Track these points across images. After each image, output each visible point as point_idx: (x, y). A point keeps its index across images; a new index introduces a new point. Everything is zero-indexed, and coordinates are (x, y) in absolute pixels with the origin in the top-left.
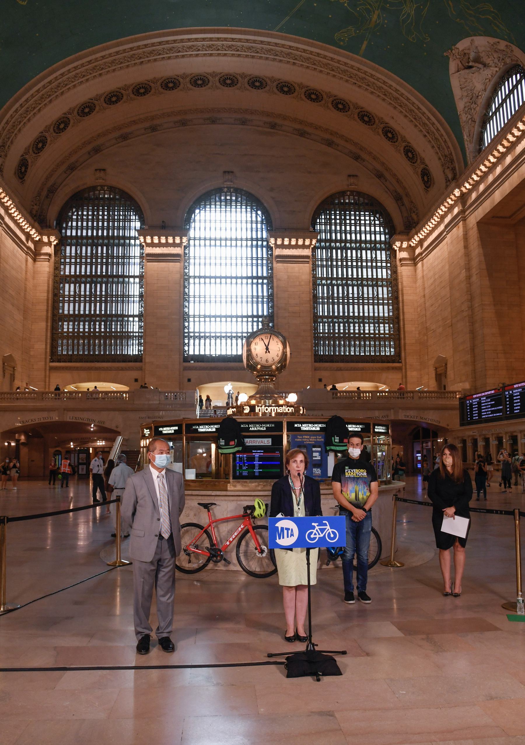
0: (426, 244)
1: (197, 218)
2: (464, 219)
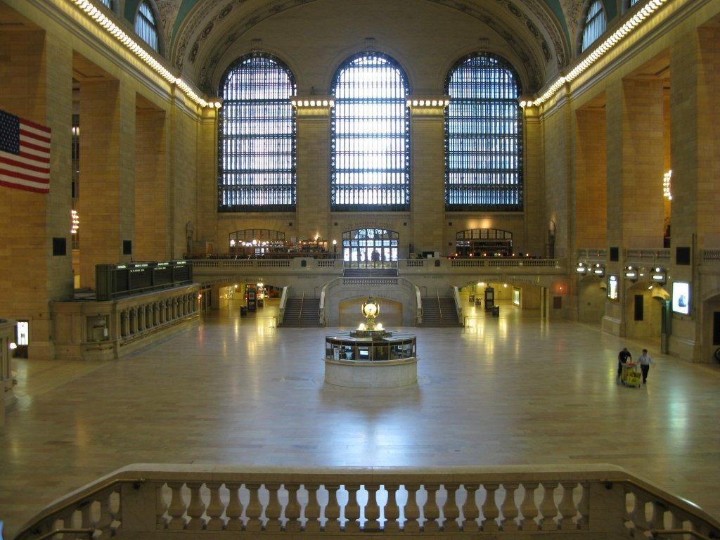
0: (546, 107)
1: (342, 81)
2: (569, 102)
